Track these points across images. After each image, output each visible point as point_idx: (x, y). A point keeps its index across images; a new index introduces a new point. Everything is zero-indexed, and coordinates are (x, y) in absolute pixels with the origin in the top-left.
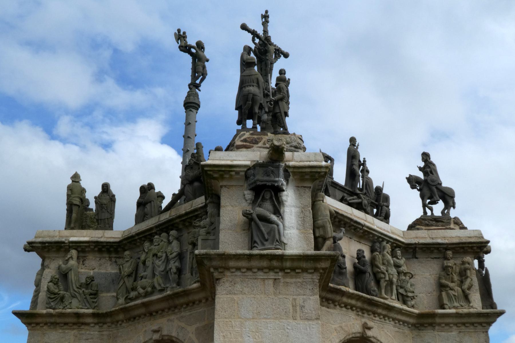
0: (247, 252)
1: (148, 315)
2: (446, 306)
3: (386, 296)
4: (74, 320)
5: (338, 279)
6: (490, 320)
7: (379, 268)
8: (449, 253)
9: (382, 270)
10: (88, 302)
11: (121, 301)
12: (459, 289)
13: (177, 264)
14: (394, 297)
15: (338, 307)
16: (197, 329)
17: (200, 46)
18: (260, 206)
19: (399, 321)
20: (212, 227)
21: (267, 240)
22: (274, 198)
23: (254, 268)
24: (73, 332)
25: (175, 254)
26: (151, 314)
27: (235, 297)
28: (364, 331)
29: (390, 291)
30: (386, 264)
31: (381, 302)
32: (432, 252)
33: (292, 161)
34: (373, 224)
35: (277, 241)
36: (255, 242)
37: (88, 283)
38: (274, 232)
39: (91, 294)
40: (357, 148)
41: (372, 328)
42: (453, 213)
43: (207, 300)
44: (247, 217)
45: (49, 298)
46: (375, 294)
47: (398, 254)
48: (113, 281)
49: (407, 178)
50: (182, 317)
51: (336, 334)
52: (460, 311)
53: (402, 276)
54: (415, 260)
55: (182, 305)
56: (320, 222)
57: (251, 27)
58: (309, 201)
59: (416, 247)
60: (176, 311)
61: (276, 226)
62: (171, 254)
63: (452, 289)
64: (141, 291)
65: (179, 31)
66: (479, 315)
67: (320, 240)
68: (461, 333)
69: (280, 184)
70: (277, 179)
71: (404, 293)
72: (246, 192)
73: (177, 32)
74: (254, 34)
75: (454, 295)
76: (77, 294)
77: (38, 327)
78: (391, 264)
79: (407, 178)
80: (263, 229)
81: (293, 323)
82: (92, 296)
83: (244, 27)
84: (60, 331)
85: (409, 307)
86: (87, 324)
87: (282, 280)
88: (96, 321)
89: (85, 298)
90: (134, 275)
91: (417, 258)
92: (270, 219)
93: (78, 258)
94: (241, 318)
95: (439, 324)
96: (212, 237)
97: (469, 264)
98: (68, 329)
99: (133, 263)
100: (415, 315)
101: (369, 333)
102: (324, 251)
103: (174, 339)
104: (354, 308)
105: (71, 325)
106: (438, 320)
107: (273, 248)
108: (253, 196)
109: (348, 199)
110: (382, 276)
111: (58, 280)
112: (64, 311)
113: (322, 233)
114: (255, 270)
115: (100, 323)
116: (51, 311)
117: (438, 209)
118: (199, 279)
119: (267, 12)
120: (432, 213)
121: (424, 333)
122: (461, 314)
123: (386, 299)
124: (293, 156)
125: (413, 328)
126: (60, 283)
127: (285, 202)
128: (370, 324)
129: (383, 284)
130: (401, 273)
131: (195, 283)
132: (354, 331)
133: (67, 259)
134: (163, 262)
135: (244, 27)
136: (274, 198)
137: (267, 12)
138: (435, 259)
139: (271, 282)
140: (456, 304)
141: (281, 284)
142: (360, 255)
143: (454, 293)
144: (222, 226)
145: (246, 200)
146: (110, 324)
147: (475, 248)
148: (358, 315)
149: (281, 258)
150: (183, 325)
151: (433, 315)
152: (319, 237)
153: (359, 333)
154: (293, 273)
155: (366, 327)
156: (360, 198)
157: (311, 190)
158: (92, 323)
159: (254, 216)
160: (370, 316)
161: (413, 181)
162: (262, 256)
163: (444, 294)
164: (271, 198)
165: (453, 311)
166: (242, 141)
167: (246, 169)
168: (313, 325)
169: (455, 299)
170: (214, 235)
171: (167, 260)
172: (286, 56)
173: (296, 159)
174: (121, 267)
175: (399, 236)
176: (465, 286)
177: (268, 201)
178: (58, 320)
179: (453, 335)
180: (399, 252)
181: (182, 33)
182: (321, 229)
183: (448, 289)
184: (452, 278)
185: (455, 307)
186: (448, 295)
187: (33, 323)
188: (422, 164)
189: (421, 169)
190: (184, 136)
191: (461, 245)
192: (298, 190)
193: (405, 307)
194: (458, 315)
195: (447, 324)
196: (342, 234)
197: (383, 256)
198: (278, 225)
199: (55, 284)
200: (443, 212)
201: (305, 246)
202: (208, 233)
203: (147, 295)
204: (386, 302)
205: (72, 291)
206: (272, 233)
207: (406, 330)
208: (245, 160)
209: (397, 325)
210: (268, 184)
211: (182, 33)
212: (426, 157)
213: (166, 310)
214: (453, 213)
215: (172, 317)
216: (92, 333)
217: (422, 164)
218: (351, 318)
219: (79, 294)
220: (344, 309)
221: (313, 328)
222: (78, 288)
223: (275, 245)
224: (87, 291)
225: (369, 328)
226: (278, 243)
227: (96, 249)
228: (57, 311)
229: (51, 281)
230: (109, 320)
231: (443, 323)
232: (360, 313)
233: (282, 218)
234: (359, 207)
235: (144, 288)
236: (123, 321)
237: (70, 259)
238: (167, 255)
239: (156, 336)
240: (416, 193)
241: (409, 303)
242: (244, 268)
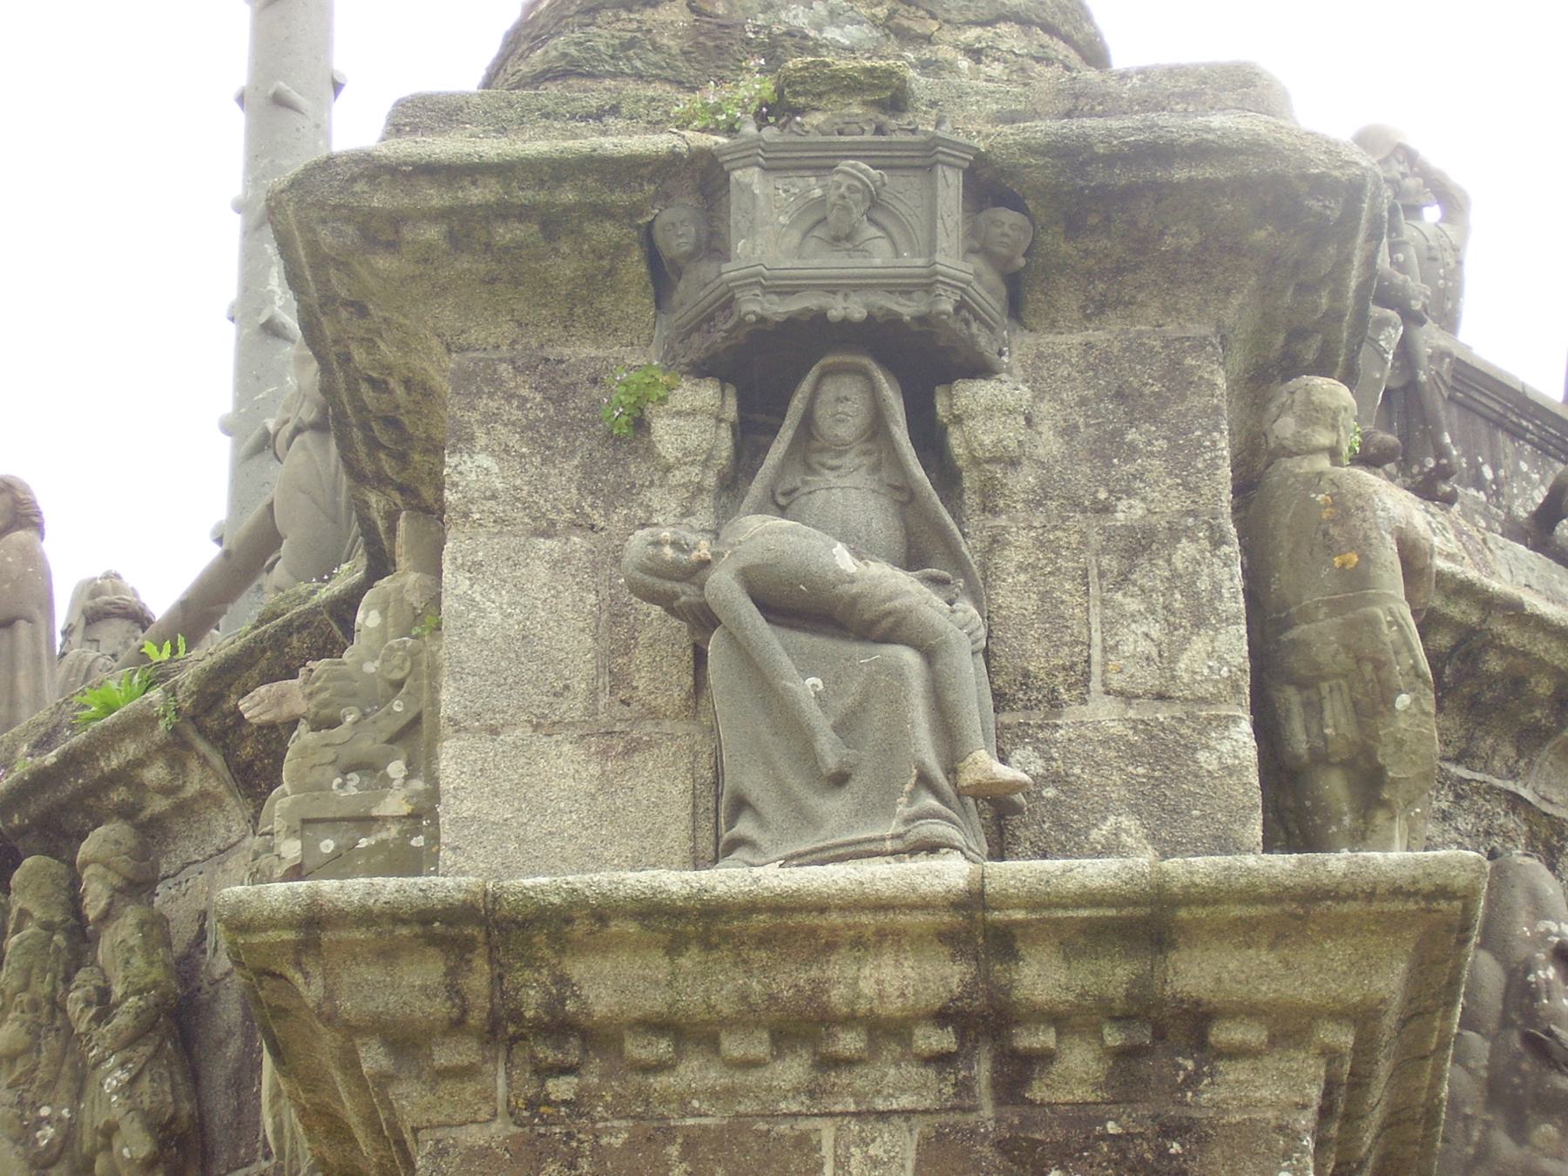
0: (676, 881)
18: (781, 503)
21: (840, 780)
35: (925, 781)
36: (740, 804)
38: (896, 700)
61: (909, 658)
69: (948, 307)
92: (854, 600)
107: (889, 845)
108: (725, 435)
159: (723, 584)
164: (877, 427)
177: (849, 460)
190: (241, 99)
198: (930, 653)
210: (844, 308)
223: (908, 821)
226: (931, 802)
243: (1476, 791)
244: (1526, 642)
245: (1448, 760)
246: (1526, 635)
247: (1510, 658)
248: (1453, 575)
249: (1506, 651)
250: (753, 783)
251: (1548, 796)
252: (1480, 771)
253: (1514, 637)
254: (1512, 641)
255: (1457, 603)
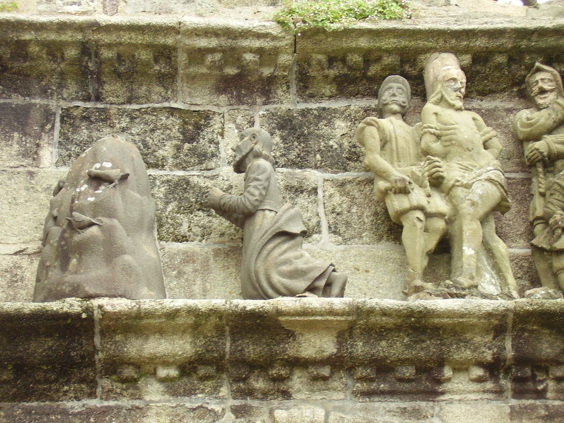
243: (146, 113)
244: (115, 38)
245: (123, 103)
246: (114, 35)
247: (115, 49)
248: (51, 22)
249: (109, 46)
251: (194, 103)
252: (146, 103)
253: (106, 38)
254: (106, 40)
255: (65, 34)
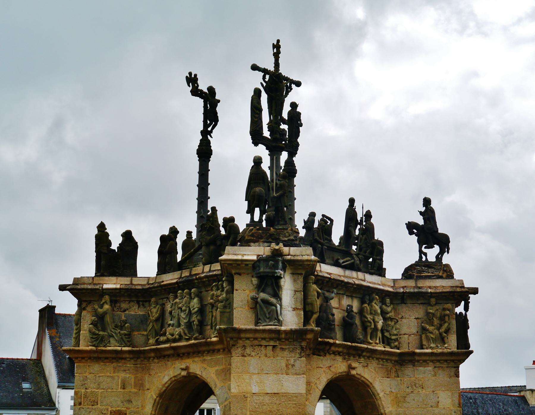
1: (176, 355)
2: (424, 347)
3: (371, 341)
4: (114, 356)
5: (327, 334)
6: (461, 358)
7: (367, 318)
8: (433, 300)
9: (369, 319)
10: (124, 342)
11: (152, 341)
12: (437, 332)
13: (198, 318)
14: (378, 341)
15: (327, 354)
16: (217, 371)
17: (211, 90)
19: (382, 359)
20: (228, 303)
22: (274, 285)
23: (259, 338)
24: (112, 365)
25: (196, 309)
26: (178, 355)
27: (246, 358)
28: (349, 371)
29: (375, 336)
30: (373, 313)
31: (364, 348)
32: (418, 299)
33: (288, 255)
34: (364, 281)
36: (260, 319)
37: (123, 325)
39: (125, 335)
40: (355, 208)
41: (356, 368)
42: (446, 259)
43: (224, 350)
44: (254, 300)
45: (92, 338)
46: (359, 341)
47: (387, 302)
48: (142, 321)
49: (406, 224)
50: (205, 360)
51: (324, 375)
52: (435, 351)
53: (388, 321)
54: (403, 305)
55: (204, 352)
56: (309, 300)
57: (262, 66)
58: (300, 285)
59: (404, 295)
60: (200, 355)
62: (193, 309)
63: (431, 333)
64: (170, 337)
65: (190, 74)
66: (452, 354)
67: (309, 313)
68: (436, 368)
70: (277, 271)
71: (388, 336)
72: (253, 279)
73: (188, 76)
74: (265, 71)
75: (432, 338)
76: (114, 334)
77: (84, 361)
78: (378, 313)
79: (406, 224)
80: (265, 310)
81: (286, 377)
82: (127, 337)
83: (255, 68)
84: (102, 364)
85: (392, 348)
86: (125, 359)
87: (279, 347)
88: (131, 356)
89: (121, 338)
90: (161, 321)
91: (405, 304)
93: (111, 301)
94: (249, 373)
95: (418, 361)
96: (228, 310)
97: (449, 310)
98: (108, 362)
99: (159, 309)
100: (397, 354)
101: (353, 372)
102: (309, 327)
103: (199, 376)
104: (341, 354)
105: (111, 359)
106: (417, 358)
109: (341, 261)
110: (369, 324)
111: (97, 322)
112: (104, 348)
113: (310, 309)
114: (260, 340)
115: (135, 358)
116: (94, 348)
117: (432, 254)
118: (217, 335)
119: (278, 41)
120: (426, 259)
121: (405, 368)
122: (436, 353)
123: (370, 343)
124: (289, 250)
125: (396, 363)
126: (99, 325)
127: (282, 287)
128: (354, 365)
129: (369, 331)
130: (388, 319)
131: (215, 337)
132: (340, 371)
133: (102, 303)
134: (187, 315)
135: (255, 68)
136: (274, 285)
137: (278, 41)
138: (421, 305)
139: (271, 348)
140: (432, 345)
141: (278, 349)
142: (349, 310)
143: (432, 336)
144: (235, 305)
145: (254, 285)
146: (143, 359)
147: (456, 296)
148: (345, 359)
149: (278, 332)
150: (205, 366)
151: (414, 354)
152: (308, 311)
153: (345, 372)
154: (287, 342)
155: (350, 367)
156: (353, 258)
157: (303, 276)
158: (128, 358)
160: (356, 358)
161: (411, 227)
162: (264, 331)
163: (423, 336)
164: (272, 284)
165: (429, 351)
166: (251, 236)
167: (253, 263)
168: (300, 378)
169: (433, 341)
170: (229, 309)
171: (190, 314)
172: (298, 84)
173: (291, 253)
174: (150, 312)
175: (389, 286)
176: (443, 330)
178: (100, 356)
179: (429, 369)
180: (388, 300)
181: (193, 76)
182: (310, 305)
183: (428, 332)
184: (433, 323)
185: (432, 348)
186: (427, 337)
187: (79, 358)
188: (423, 209)
189: (421, 213)
191: (443, 294)
192: (293, 276)
193: (388, 349)
194: (432, 354)
195: (425, 361)
196: (333, 295)
197: (372, 306)
199: (94, 326)
200: (437, 257)
201: (297, 320)
202: (225, 307)
203: (175, 341)
204: (370, 347)
205: (109, 332)
206: (272, 313)
207: (390, 365)
208: (253, 254)
209: (381, 362)
210: (270, 274)
211: (193, 76)
212: (427, 202)
213: (191, 354)
214: (446, 259)
215: (196, 359)
216: (128, 365)
217: (423, 209)
218: (339, 361)
219: (115, 333)
220: (333, 355)
221: (300, 380)
222: (114, 329)
223: (274, 323)
224: (122, 332)
225: (354, 368)
226: (276, 321)
227: (126, 294)
228: (100, 348)
229: (91, 324)
230: (142, 356)
231: (421, 360)
232: (346, 357)
233: (281, 300)
234: (352, 267)
235: (172, 335)
236: (154, 358)
237: (105, 304)
238: (190, 309)
239: (184, 373)
240: (414, 238)
241: (392, 345)
242: (251, 338)
250: (261, 318)
